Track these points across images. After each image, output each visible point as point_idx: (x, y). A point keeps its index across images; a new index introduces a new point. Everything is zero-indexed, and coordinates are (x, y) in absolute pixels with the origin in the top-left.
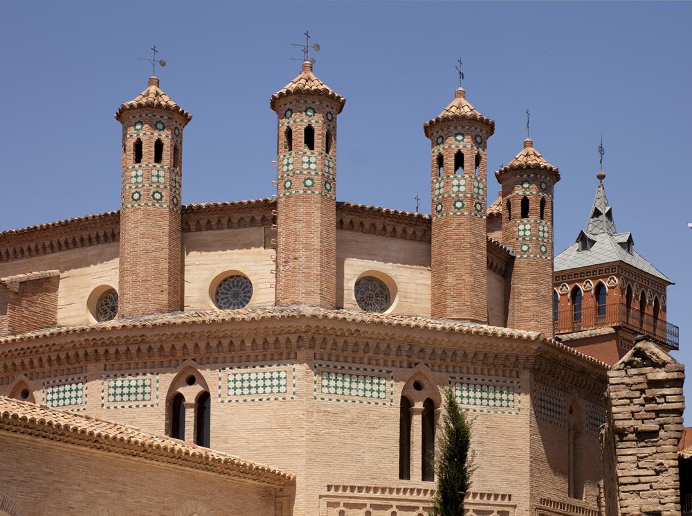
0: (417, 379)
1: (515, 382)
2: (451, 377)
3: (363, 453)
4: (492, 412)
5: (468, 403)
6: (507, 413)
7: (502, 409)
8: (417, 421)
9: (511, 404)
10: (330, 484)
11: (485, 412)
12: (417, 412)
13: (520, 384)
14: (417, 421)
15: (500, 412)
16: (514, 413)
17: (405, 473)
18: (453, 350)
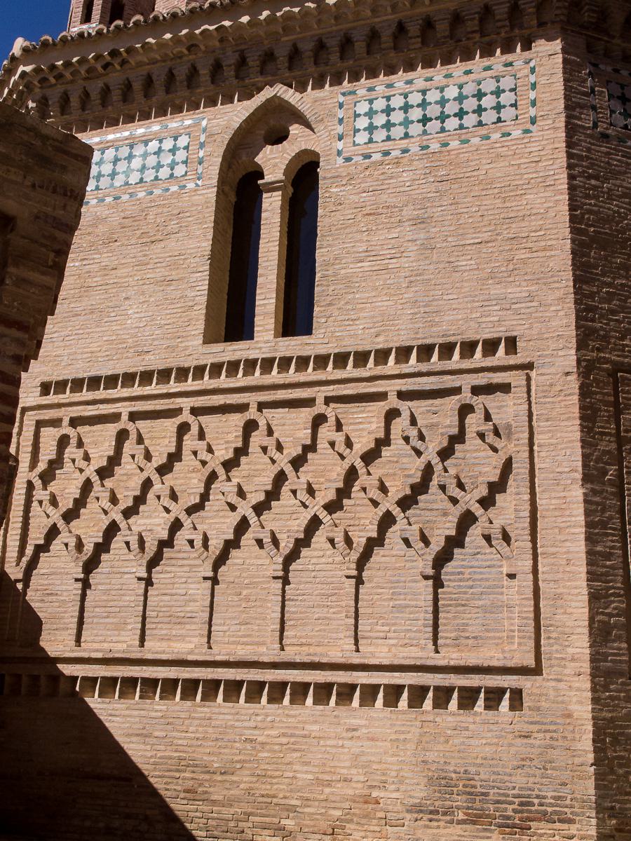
0: (272, 122)
1: (518, 64)
2: (344, 94)
3: (127, 298)
4: (454, 144)
5: (389, 138)
6: (496, 136)
7: (483, 131)
8: (272, 208)
9: (508, 113)
10: (46, 379)
11: (435, 146)
12: (271, 188)
13: (532, 64)
14: (272, 208)
15: (475, 141)
16: (517, 133)
17: (233, 318)
18: (342, 33)
